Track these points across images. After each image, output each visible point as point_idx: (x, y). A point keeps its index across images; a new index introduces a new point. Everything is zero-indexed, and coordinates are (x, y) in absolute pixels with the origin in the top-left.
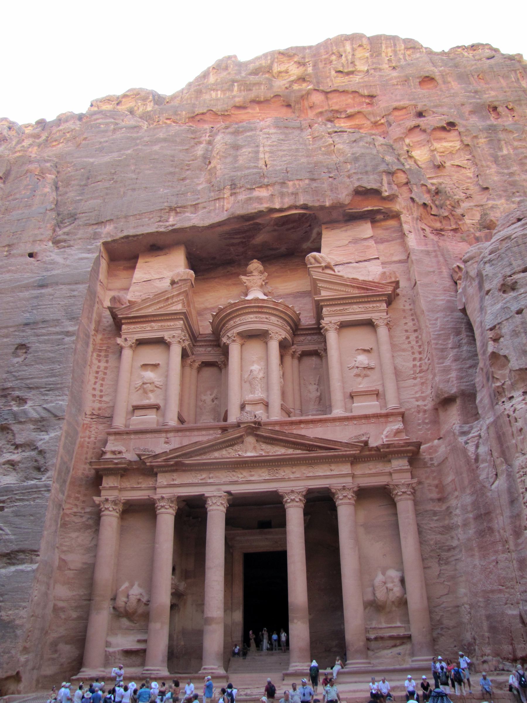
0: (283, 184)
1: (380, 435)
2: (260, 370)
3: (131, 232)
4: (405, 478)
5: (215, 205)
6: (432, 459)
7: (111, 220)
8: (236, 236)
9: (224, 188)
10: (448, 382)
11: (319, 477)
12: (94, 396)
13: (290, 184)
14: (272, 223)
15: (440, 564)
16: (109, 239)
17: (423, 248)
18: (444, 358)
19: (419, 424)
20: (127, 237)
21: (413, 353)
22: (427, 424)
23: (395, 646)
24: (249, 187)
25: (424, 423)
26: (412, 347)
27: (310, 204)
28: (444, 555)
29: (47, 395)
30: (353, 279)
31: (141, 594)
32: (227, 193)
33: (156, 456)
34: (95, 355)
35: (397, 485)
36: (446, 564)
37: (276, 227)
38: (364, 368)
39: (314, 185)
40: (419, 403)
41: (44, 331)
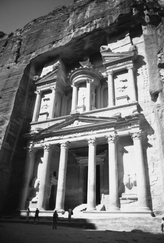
0: (91, 22)
1: (126, 113)
2: (83, 95)
3: (40, 53)
4: (138, 130)
5: (68, 37)
6: (150, 122)
7: (34, 51)
8: (77, 47)
9: (71, 30)
10: (155, 86)
11: (101, 133)
12: (28, 113)
13: (95, 21)
14: (89, 39)
15: (153, 167)
16: (34, 58)
17: (151, 34)
18: (154, 77)
19: (145, 108)
20: (39, 55)
21: (144, 78)
22: (149, 107)
23: (131, 202)
24: (79, 26)
25: (148, 107)
26: (144, 76)
27: (101, 27)
28: (156, 163)
29: (6, 113)
30: (118, 53)
31: (39, 181)
32: (72, 31)
33: (43, 130)
34: (29, 99)
35: (133, 134)
36: (157, 167)
37: (91, 40)
38: (123, 88)
39: (103, 19)
40: (145, 99)
41: (7, 92)
